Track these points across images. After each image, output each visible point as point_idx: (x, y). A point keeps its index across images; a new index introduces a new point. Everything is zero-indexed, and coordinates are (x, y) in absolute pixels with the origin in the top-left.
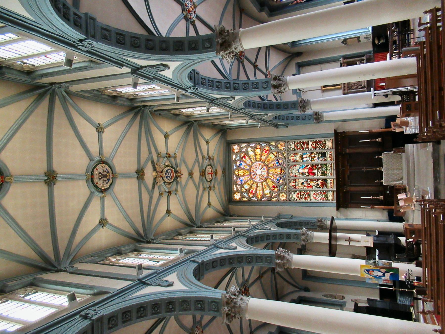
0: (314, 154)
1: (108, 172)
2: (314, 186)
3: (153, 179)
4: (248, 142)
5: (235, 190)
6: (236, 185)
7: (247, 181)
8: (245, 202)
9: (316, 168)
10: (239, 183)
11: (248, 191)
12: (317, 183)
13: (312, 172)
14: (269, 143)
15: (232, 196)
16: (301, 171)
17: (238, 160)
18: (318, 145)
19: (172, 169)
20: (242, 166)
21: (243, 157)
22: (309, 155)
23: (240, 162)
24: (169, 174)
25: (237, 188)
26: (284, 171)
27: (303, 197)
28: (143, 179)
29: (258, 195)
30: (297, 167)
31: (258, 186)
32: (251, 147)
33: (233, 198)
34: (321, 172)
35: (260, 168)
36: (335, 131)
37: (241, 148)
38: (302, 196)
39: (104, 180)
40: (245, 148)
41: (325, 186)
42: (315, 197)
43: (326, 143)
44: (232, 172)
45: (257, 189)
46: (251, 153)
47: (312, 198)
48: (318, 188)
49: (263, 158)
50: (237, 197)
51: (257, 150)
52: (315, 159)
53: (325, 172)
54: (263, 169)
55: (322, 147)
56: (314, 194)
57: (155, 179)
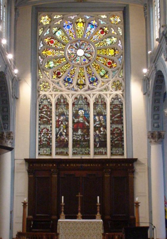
0: (103, 132)
2: (60, 130)
4: (126, 37)
5: (55, 17)
6: (62, 19)
7: (66, 35)
8: (36, 31)
9: (85, 133)
10: (65, 24)
11: (53, 36)
12: (64, 133)
13: (79, 127)
14: (122, 68)
15: (47, 13)
16: (81, 112)
17: (99, 23)
18: (116, 137)
20: (89, 28)
21: (103, 30)
22: (103, 124)
23: (96, 26)
25: (57, 20)
26: (81, 89)
27: (43, 115)
29: (47, 50)
30: (86, 107)
31: (61, 52)
32: (117, 42)
33: (44, 13)
34: (78, 139)
36: (136, 160)
37: (115, 27)
38: (44, 112)
40: (116, 33)
41: (59, 144)
42: (44, 131)
43: (119, 147)
44: (81, 13)
45: (56, 49)
46: (109, 41)
47: (42, 127)
48: (56, 135)
49: (101, 60)
50: (45, 20)
51: (113, 51)
52: (97, 132)
53: (78, 146)
54: (85, 58)
55: (114, 142)
56: (48, 130)
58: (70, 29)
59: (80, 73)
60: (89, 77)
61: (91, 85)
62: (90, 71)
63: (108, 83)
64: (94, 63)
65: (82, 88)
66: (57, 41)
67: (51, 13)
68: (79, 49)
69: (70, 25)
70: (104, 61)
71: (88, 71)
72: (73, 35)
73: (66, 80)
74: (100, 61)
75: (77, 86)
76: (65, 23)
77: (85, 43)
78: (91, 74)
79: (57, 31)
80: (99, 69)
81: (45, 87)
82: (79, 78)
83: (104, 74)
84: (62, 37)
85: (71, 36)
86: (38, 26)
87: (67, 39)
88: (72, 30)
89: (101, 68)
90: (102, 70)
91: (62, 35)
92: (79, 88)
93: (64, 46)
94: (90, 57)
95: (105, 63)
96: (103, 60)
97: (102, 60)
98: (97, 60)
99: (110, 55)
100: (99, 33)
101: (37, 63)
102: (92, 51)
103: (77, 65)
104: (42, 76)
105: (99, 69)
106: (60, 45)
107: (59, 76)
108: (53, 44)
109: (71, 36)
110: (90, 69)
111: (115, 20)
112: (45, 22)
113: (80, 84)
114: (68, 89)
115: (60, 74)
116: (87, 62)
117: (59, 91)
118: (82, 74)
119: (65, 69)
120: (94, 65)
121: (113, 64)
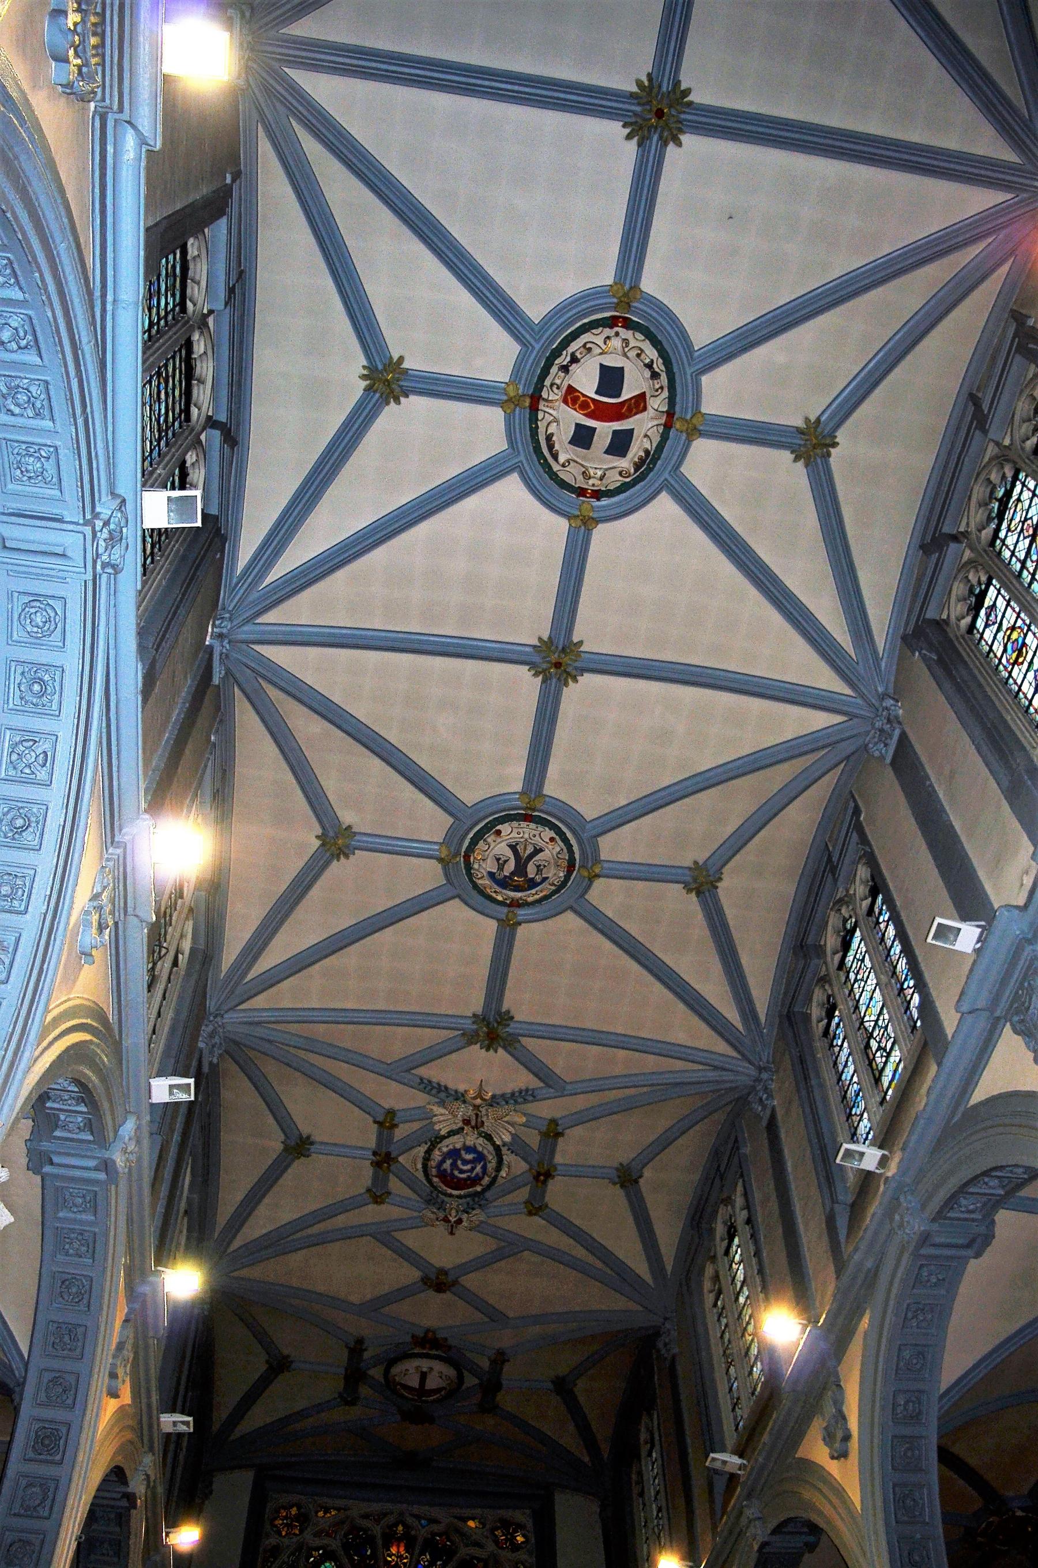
1: (532, 884)
3: (461, 1088)
19: (486, 1180)
24: (465, 1162)
28: (470, 1038)
39: (506, 861)
57: (460, 1097)
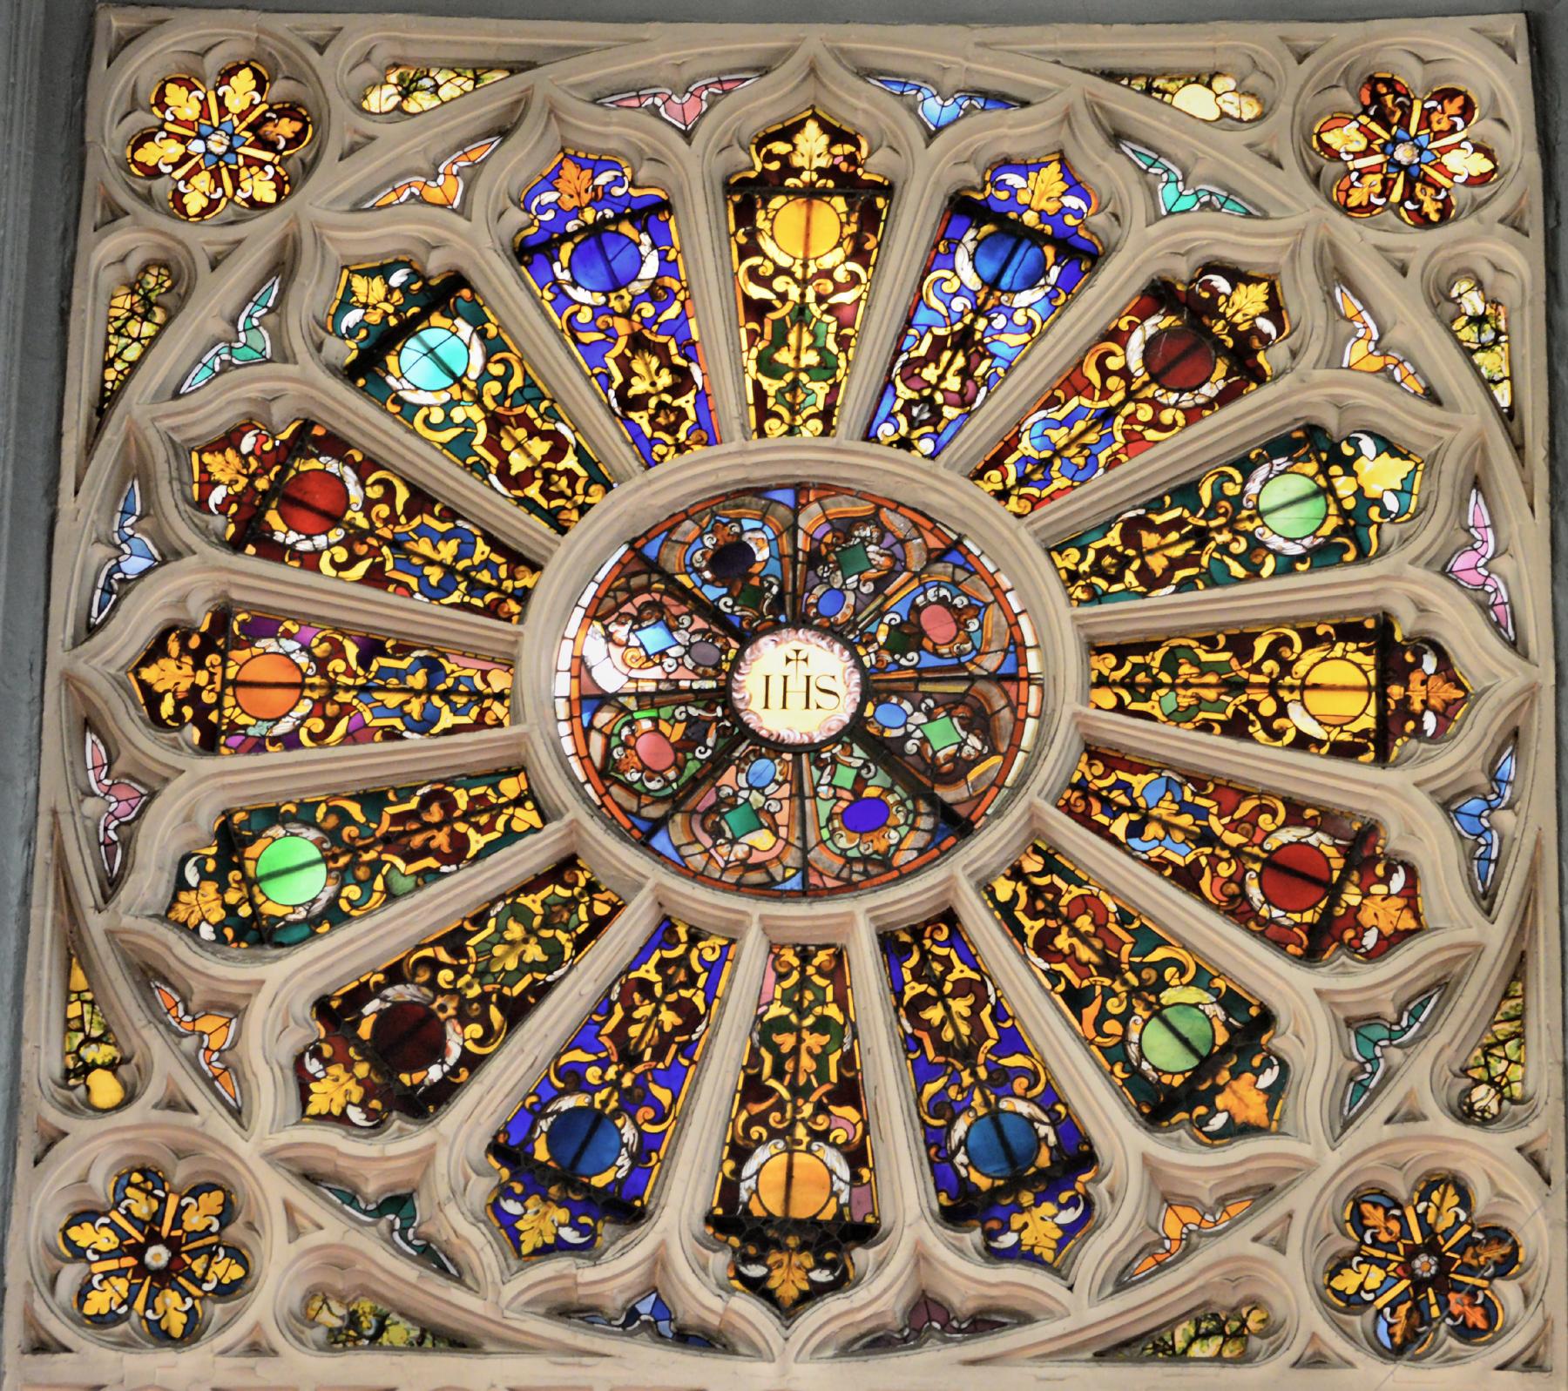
26: (787, 1311)
35: (891, 719)
58: (638, 288)
59: (781, 1024)
60: (944, 1108)
61: (974, 1237)
62: (961, 1006)
63: (1289, 160)
64: (1033, 864)
65: (814, 1293)
66: (402, 495)
67: (317, 24)
68: (776, 627)
69: (626, 228)
70: (1206, 838)
71: (922, 1001)
72: (676, 390)
73: (541, 1153)
74: (1135, 830)
75: (720, 1261)
76: (548, 197)
77: (883, 530)
78: (966, 1053)
79: (408, 329)
80: (1110, 967)
81: (157, 1256)
82: (761, 1119)
83: (1207, 1064)
84: (496, 423)
85: (639, 402)
86: (86, 225)
87: (570, 461)
88: (672, 312)
89: (1159, 954)
90: (1167, 997)
91: (494, 388)
92: (757, 1287)
93: (527, 580)
94: (960, 767)
95: (1224, 870)
96: (1186, 820)
97: (1167, 827)
98: (1085, 820)
99: (1303, 742)
100: (1125, 373)
101: (43, 852)
102: (991, 663)
103: (739, 888)
104: (112, 1067)
105: (1110, 967)
106: (448, 550)
107: (405, 1078)
108: (337, 534)
109: (641, 418)
110: (961, 971)
111: (1403, 154)
112: (203, 181)
113: (769, 1219)
114: (569, 1311)
115: (437, 1051)
116: (917, 840)
117: (398, 1332)
118: (821, 1059)
119: (524, 968)
120: (1035, 892)
121: (1352, 897)
